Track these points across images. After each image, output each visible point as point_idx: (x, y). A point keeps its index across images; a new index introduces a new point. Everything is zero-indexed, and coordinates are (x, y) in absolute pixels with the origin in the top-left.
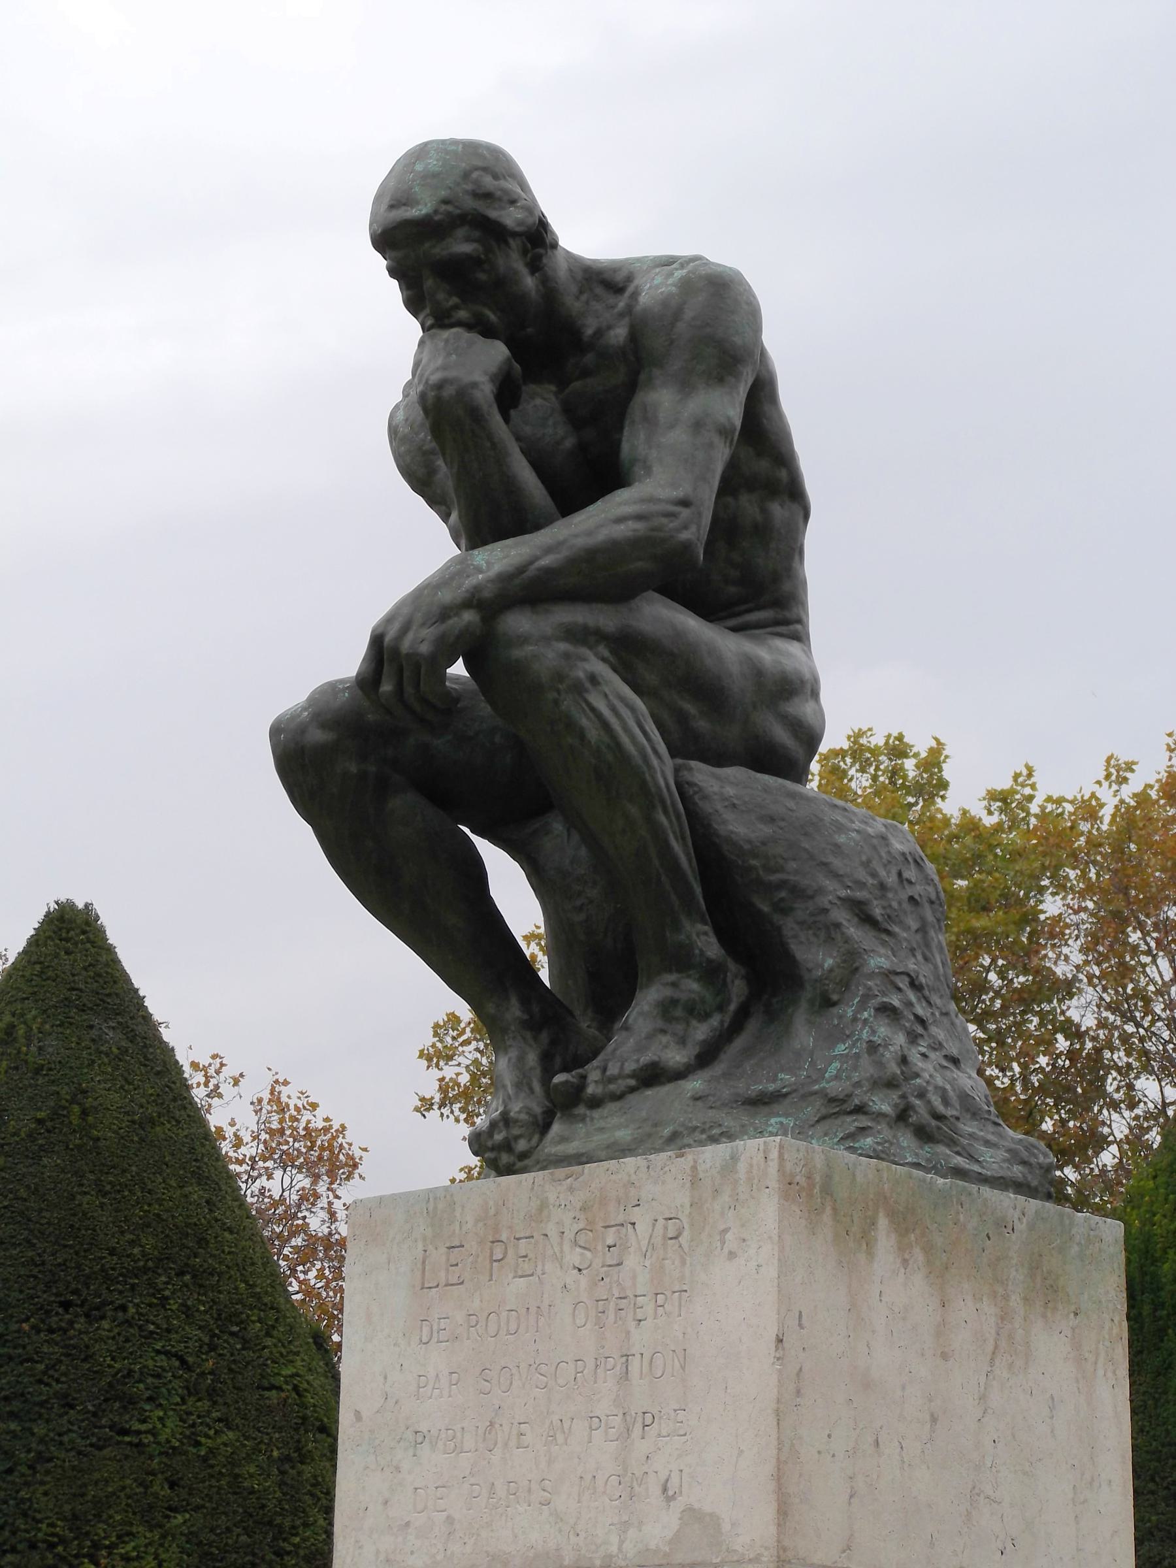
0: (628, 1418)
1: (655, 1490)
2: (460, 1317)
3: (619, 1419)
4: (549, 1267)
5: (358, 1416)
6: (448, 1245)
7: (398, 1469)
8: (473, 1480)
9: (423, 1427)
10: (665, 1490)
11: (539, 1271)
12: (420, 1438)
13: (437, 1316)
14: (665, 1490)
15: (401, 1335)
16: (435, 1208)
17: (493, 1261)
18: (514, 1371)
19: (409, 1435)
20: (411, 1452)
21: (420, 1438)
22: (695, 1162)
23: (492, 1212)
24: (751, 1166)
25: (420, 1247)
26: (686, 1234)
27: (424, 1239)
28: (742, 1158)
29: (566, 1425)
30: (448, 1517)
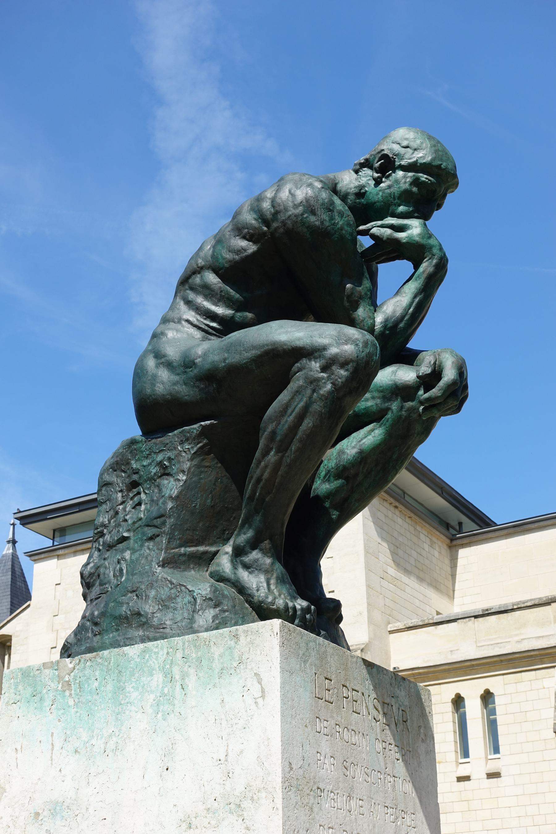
13: (323, 717)
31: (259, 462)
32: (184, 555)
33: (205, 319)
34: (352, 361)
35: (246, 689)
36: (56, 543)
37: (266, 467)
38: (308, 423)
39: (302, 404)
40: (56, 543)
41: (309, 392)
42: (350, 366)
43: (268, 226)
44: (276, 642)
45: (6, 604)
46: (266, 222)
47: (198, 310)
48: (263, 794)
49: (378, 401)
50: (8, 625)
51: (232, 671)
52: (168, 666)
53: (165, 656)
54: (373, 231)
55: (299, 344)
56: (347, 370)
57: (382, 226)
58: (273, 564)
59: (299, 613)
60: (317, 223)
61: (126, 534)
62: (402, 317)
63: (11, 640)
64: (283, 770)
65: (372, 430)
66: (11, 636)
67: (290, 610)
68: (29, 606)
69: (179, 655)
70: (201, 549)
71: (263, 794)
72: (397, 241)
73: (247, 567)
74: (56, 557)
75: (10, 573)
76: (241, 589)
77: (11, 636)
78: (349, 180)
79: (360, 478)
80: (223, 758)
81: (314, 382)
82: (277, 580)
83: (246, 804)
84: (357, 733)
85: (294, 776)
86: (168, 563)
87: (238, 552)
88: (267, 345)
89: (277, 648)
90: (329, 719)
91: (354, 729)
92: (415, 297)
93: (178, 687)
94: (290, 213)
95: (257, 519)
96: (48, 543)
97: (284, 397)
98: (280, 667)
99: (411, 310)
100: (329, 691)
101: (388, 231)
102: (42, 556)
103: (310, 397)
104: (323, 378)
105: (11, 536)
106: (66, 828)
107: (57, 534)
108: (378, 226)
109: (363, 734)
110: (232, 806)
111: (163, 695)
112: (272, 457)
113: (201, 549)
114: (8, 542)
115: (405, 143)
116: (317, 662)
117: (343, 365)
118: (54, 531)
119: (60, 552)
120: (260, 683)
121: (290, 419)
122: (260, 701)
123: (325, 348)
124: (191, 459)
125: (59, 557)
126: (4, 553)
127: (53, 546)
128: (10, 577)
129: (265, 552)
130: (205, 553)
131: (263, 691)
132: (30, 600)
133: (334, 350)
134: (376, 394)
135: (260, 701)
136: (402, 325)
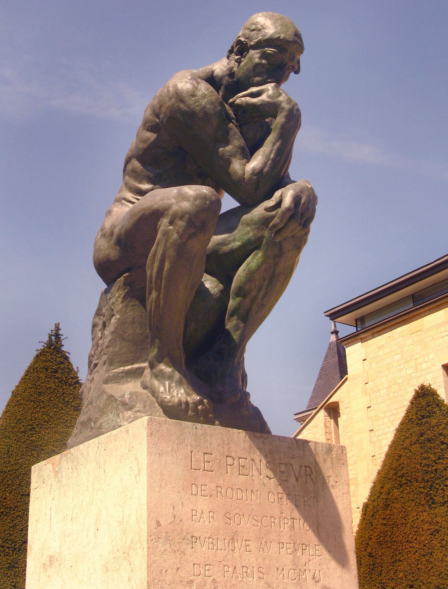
0: (296, 545)
2: (213, 486)
3: (292, 545)
4: (255, 473)
5: (158, 524)
6: (204, 451)
7: (183, 553)
8: (225, 564)
9: (196, 534)
10: (314, 577)
11: (251, 474)
12: (194, 539)
13: (200, 483)
15: (181, 488)
16: (196, 433)
17: (227, 465)
18: (242, 516)
19: (189, 536)
20: (190, 545)
21: (194, 539)
22: (316, 446)
23: (226, 442)
24: (337, 454)
25: (189, 448)
26: (314, 474)
27: (191, 445)
28: (334, 450)
29: (269, 544)
30: (213, 580)
31: (149, 299)
32: (122, 372)
33: (136, 195)
34: (186, 213)
35: (131, 469)
36: (359, 329)
37: (152, 301)
38: (167, 266)
39: (161, 252)
40: (359, 329)
41: (163, 241)
42: (184, 219)
43: (158, 118)
44: (144, 433)
45: (338, 378)
46: (157, 116)
48: (139, 545)
49: (255, 232)
51: (126, 457)
52: (98, 456)
53: (97, 449)
54: (238, 101)
55: (156, 207)
56: (184, 221)
58: (173, 371)
59: (190, 406)
60: (185, 108)
61: (96, 362)
62: (265, 164)
63: (339, 405)
64: (149, 526)
65: (257, 254)
66: (338, 402)
67: (183, 405)
68: (347, 379)
69: (103, 448)
70: (136, 366)
71: (139, 545)
72: (254, 105)
73: (156, 376)
74: (360, 340)
75: (337, 355)
76: (154, 393)
77: (338, 402)
78: (220, 67)
79: (254, 293)
80: (121, 521)
81: (166, 233)
82: (176, 383)
83: (132, 553)
84: (244, 490)
85: (162, 530)
86: (110, 381)
87: (152, 366)
88: (140, 212)
89: (146, 438)
90: (208, 484)
91: (240, 487)
92: (274, 145)
93: (103, 471)
94: (167, 105)
95: (157, 341)
96: (353, 330)
98: (147, 452)
99: (272, 156)
100: (209, 462)
101: (248, 99)
102: (350, 341)
103: (165, 246)
104: (171, 230)
105: (333, 328)
106: (56, 574)
107: (359, 323)
108: (241, 97)
109: (252, 491)
110: (125, 554)
112: (154, 294)
113: (136, 366)
114: (332, 333)
116: (193, 443)
117: (181, 218)
118: (356, 320)
119: (362, 336)
120: (138, 464)
121: (156, 265)
122: (138, 477)
124: (122, 302)
125: (363, 340)
126: (331, 341)
127: (357, 331)
128: (337, 358)
129: (167, 365)
131: (139, 471)
132: (347, 374)
133: (175, 208)
134: (253, 227)
135: (138, 477)
136: (266, 170)
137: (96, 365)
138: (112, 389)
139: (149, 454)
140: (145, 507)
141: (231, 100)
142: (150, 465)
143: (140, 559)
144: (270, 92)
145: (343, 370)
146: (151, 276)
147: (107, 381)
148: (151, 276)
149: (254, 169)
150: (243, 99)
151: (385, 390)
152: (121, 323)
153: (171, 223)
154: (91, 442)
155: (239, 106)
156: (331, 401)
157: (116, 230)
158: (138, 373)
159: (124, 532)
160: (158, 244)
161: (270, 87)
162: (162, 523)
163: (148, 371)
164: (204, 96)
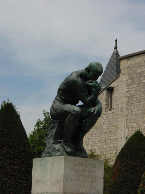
1: (93, 188)
14: (94, 188)
47: (60, 97)
50: (112, 84)
57: (89, 82)
63: (113, 88)
68: (119, 76)
70: (60, 140)
76: (64, 148)
83: (60, 182)
87: (64, 142)
97: (67, 120)
101: (89, 83)
111: (51, 165)
113: (60, 140)
115: (92, 66)
121: (67, 123)
123: (71, 112)
130: (60, 141)
133: (72, 113)
137: (49, 138)
138: (54, 146)
139: (64, 163)
140: (63, 174)
141: (85, 82)
142: (64, 166)
143: (61, 184)
144: (94, 83)
145: (118, 71)
146: (66, 125)
147: (53, 144)
148: (66, 125)
149: (89, 100)
150: (88, 83)
151: (136, 85)
152: (57, 130)
153: (71, 116)
154: (50, 157)
155: (87, 85)
156: (110, 86)
157: (58, 111)
158: (60, 142)
159: (58, 178)
160: (68, 119)
161: (94, 81)
162: (66, 177)
163: (63, 143)
164: (79, 83)
